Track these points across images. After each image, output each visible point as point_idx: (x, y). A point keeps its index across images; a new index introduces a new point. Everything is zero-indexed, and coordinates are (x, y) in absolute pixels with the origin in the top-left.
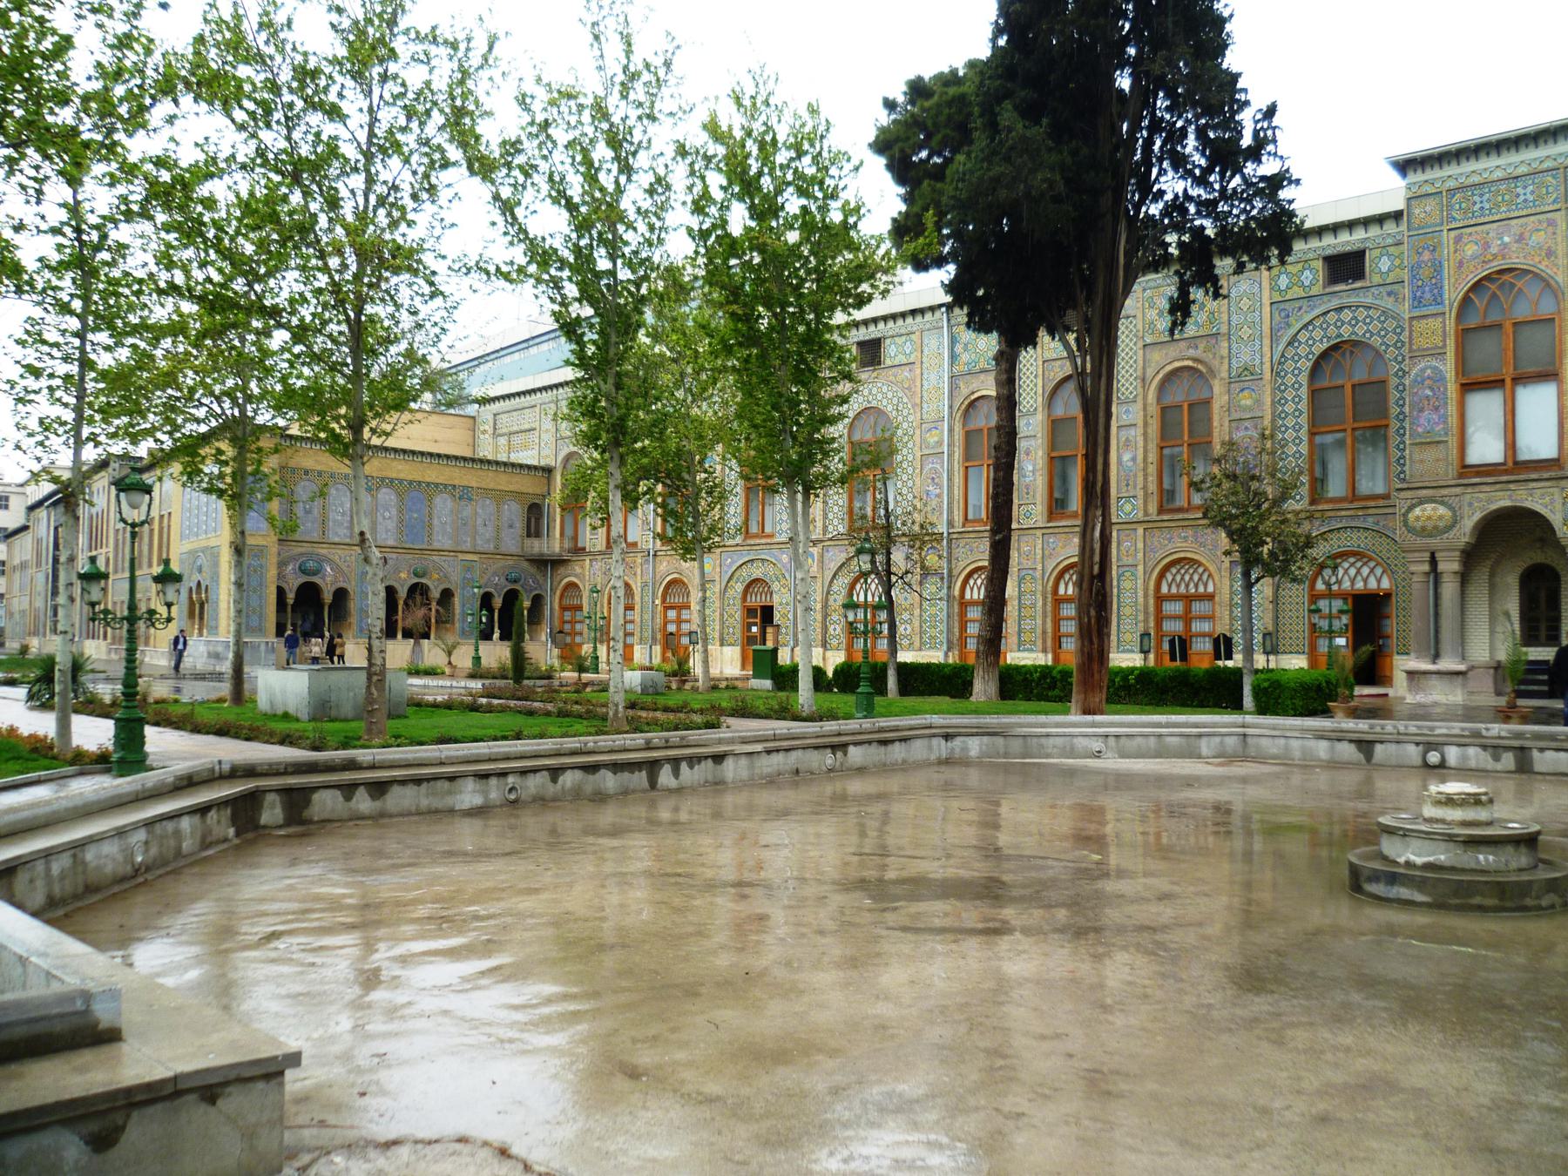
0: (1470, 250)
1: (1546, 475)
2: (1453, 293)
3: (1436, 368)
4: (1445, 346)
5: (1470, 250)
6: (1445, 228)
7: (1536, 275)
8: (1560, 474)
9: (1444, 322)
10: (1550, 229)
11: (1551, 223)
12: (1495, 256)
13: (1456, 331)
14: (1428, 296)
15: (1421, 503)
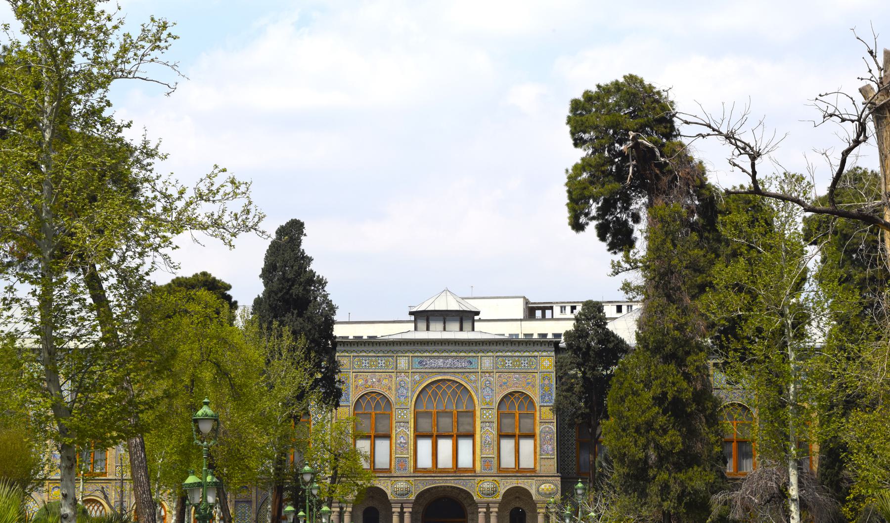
0: (361, 382)
1: (386, 475)
5: (361, 382)
6: (351, 371)
7: (384, 395)
8: (391, 475)
9: (349, 410)
10: (390, 379)
11: (391, 377)
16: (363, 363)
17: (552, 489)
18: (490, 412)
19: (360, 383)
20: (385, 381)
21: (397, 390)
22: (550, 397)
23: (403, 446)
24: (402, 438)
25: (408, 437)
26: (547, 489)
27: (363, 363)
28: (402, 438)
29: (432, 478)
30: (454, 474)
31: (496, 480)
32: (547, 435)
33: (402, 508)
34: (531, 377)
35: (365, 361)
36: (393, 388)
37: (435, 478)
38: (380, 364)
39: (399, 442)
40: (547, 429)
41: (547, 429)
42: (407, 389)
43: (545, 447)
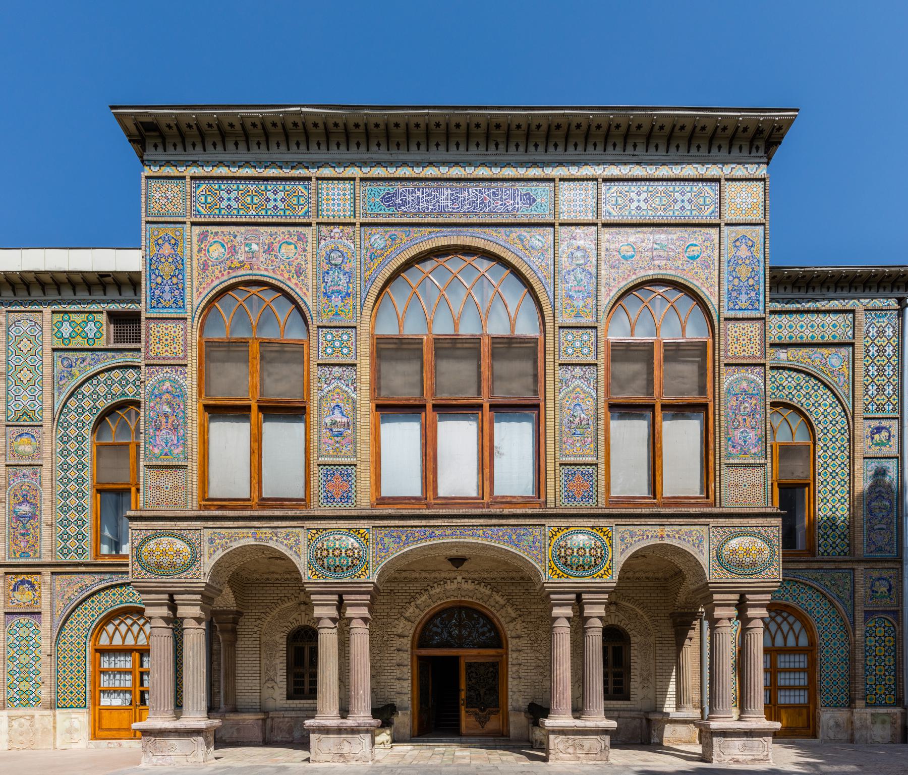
0: (216, 252)
2: (195, 298)
3: (175, 381)
4: (185, 357)
8: (305, 513)
9: (185, 330)
10: (300, 244)
11: (301, 238)
12: (242, 265)
13: (200, 343)
14: (167, 296)
15: (156, 536)
16: (221, 199)
17: (760, 551)
18: (585, 337)
19: (215, 255)
20: (288, 251)
21: (322, 275)
22: (753, 294)
23: (337, 432)
24: (336, 412)
25: (355, 409)
26: (747, 552)
27: (221, 199)
28: (336, 412)
29: (424, 522)
30: (485, 511)
31: (601, 528)
32: (744, 401)
33: (341, 606)
34: (700, 239)
35: (229, 192)
36: (310, 270)
37: (432, 522)
38: (272, 203)
39: (328, 421)
40: (744, 384)
41: (744, 384)
42: (349, 275)
43: (737, 434)
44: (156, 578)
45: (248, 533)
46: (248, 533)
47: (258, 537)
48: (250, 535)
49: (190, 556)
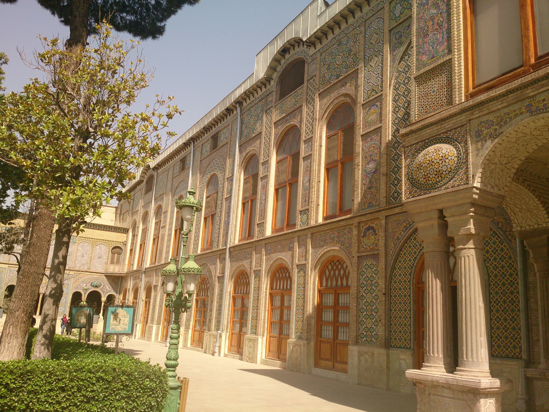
44: (425, 194)
45: (520, 109)
46: (520, 109)
47: (534, 108)
48: (524, 110)
49: (456, 159)
